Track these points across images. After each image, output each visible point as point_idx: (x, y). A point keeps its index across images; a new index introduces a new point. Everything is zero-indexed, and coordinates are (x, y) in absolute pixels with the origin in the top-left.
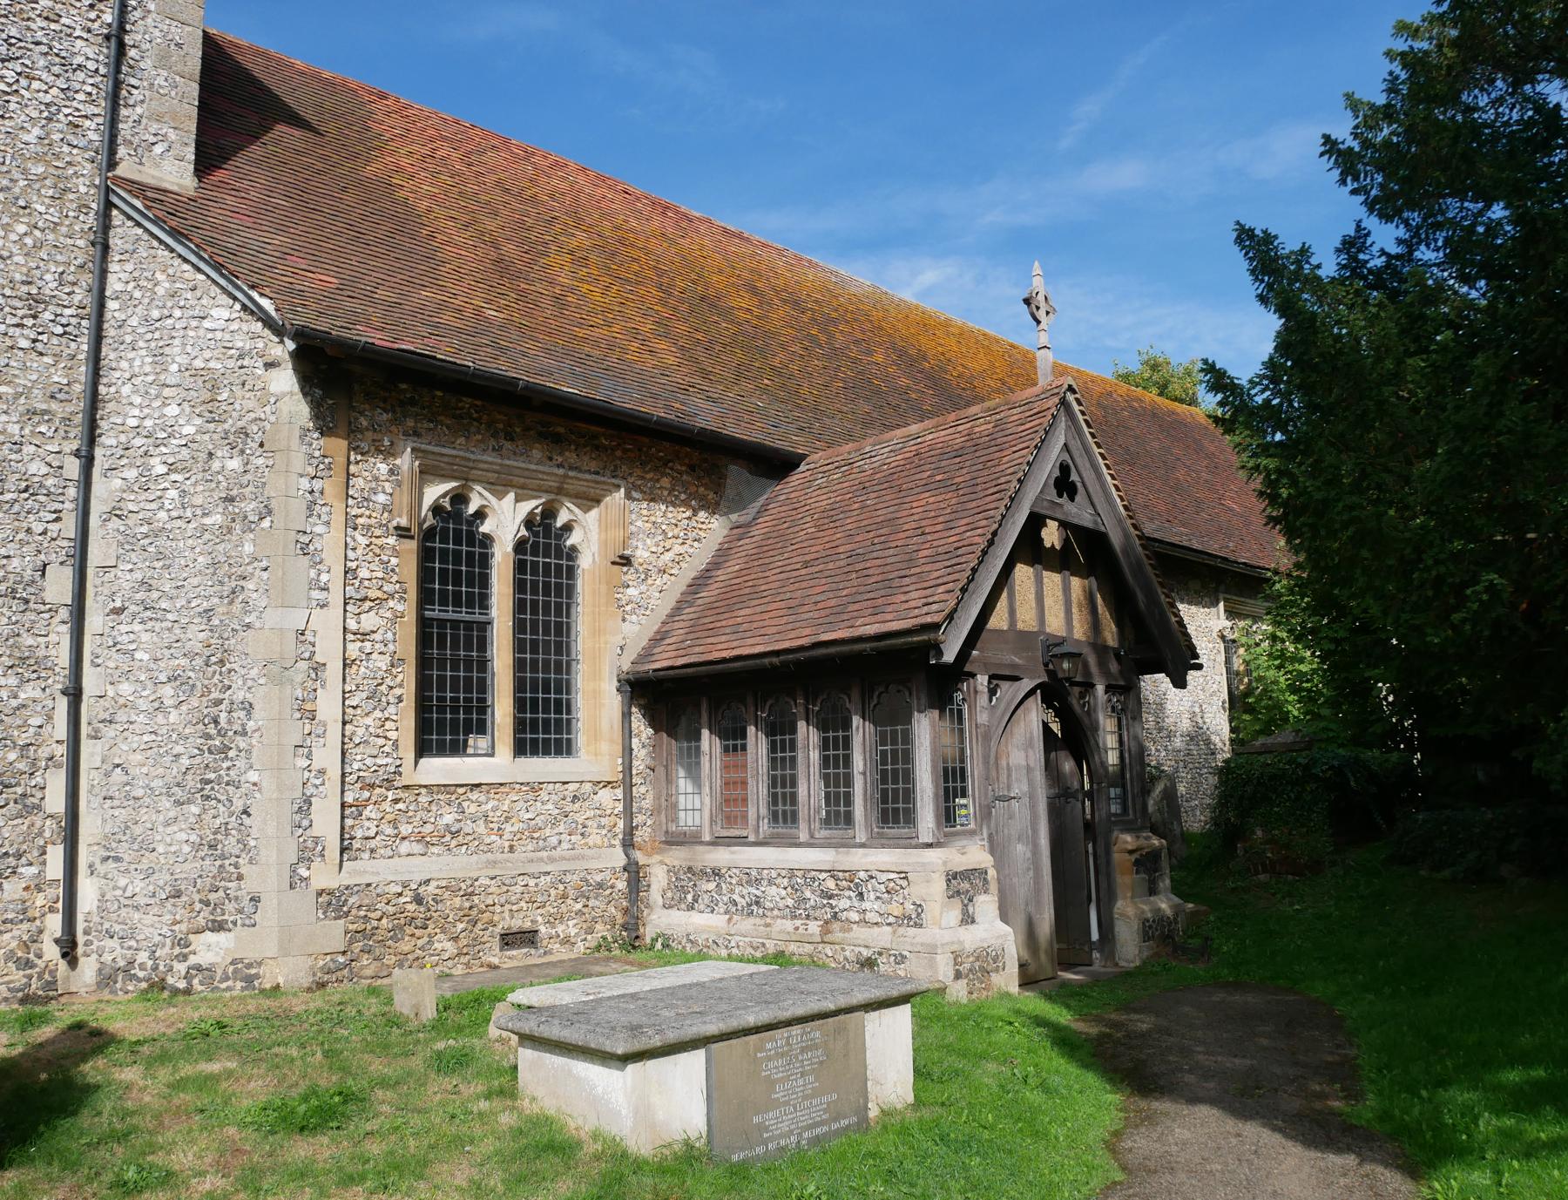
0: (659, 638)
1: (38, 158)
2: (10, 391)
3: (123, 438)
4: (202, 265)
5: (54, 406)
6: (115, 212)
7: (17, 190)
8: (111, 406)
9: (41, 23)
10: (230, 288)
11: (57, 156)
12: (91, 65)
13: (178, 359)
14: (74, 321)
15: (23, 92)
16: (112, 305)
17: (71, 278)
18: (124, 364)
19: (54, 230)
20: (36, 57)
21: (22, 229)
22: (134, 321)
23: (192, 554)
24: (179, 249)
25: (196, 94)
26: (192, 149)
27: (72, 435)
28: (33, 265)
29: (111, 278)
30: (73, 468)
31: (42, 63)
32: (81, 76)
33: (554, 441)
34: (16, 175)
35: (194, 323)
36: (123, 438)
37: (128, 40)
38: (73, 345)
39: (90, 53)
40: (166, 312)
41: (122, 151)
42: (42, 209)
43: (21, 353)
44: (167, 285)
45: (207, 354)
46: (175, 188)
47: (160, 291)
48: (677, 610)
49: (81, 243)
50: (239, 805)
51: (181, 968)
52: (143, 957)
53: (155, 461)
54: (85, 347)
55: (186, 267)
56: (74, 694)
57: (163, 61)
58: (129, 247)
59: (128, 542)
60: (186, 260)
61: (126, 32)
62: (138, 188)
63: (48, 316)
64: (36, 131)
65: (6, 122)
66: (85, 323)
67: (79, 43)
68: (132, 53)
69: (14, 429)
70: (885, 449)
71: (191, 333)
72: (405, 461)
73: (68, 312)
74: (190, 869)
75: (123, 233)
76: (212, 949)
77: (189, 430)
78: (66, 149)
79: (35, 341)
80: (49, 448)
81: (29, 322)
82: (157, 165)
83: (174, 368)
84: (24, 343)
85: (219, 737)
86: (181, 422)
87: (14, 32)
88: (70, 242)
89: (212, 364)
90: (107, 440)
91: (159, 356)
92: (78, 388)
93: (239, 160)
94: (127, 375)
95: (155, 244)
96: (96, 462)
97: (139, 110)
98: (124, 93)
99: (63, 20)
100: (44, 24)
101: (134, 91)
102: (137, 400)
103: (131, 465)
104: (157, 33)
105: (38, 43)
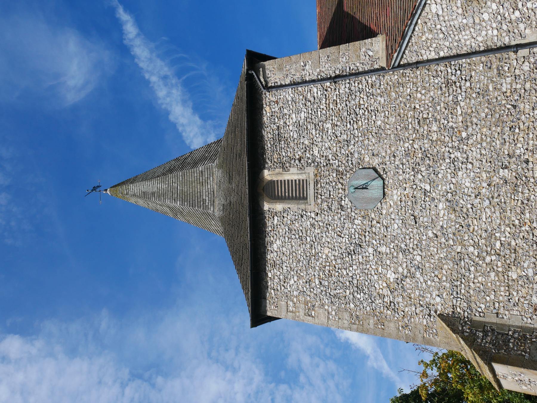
1: (389, 96)
2: (491, 85)
3: (504, 34)
4: (414, 22)
5: (494, 66)
6: (402, 63)
7: (404, 100)
8: (489, 43)
9: (339, 106)
10: (421, 7)
11: (386, 89)
12: (348, 85)
13: (460, 21)
14: (453, 67)
15: (366, 106)
16: (442, 54)
17: (434, 73)
18: (468, 43)
19: (416, 84)
20: (351, 105)
21: (419, 95)
22: (447, 44)
24: (409, 34)
25: (344, 45)
26: (366, 41)
27: (507, 56)
28: (433, 88)
29: (430, 57)
30: (523, 52)
31: (353, 102)
32: (353, 88)
34: (398, 102)
35: (441, 18)
36: (504, 34)
37: (333, 75)
38: (464, 65)
39: (343, 87)
40: (439, 31)
41: (376, 66)
42: (409, 90)
43: (473, 84)
44: (427, 34)
45: (455, 8)
46: (384, 43)
47: (430, 36)
49: (418, 73)
53: (513, 17)
54: (464, 60)
55: (417, 29)
57: (336, 61)
58: (415, 54)
60: (414, 30)
61: (331, 77)
62: (389, 57)
63: (453, 78)
64: (379, 98)
65: (379, 109)
66: (453, 63)
67: (341, 91)
68: (337, 72)
69: (509, 80)
71: (446, 18)
73: (449, 71)
75: (410, 57)
77: (494, 6)
78: (382, 87)
79: (466, 80)
80: (515, 64)
81: (458, 84)
82: (377, 52)
83: (465, 21)
84: (468, 84)
86: (491, 11)
87: (345, 114)
88: (419, 77)
89: (459, 5)
90: (507, 41)
91: (461, 29)
92: (483, 59)
93: (364, 21)
94: (473, 40)
95: (410, 44)
96: (518, 42)
97: (358, 65)
98: (353, 72)
99: (335, 98)
100: (339, 105)
101: (351, 68)
102: (484, 33)
103: (517, 27)
104: (327, 66)
105: (347, 105)
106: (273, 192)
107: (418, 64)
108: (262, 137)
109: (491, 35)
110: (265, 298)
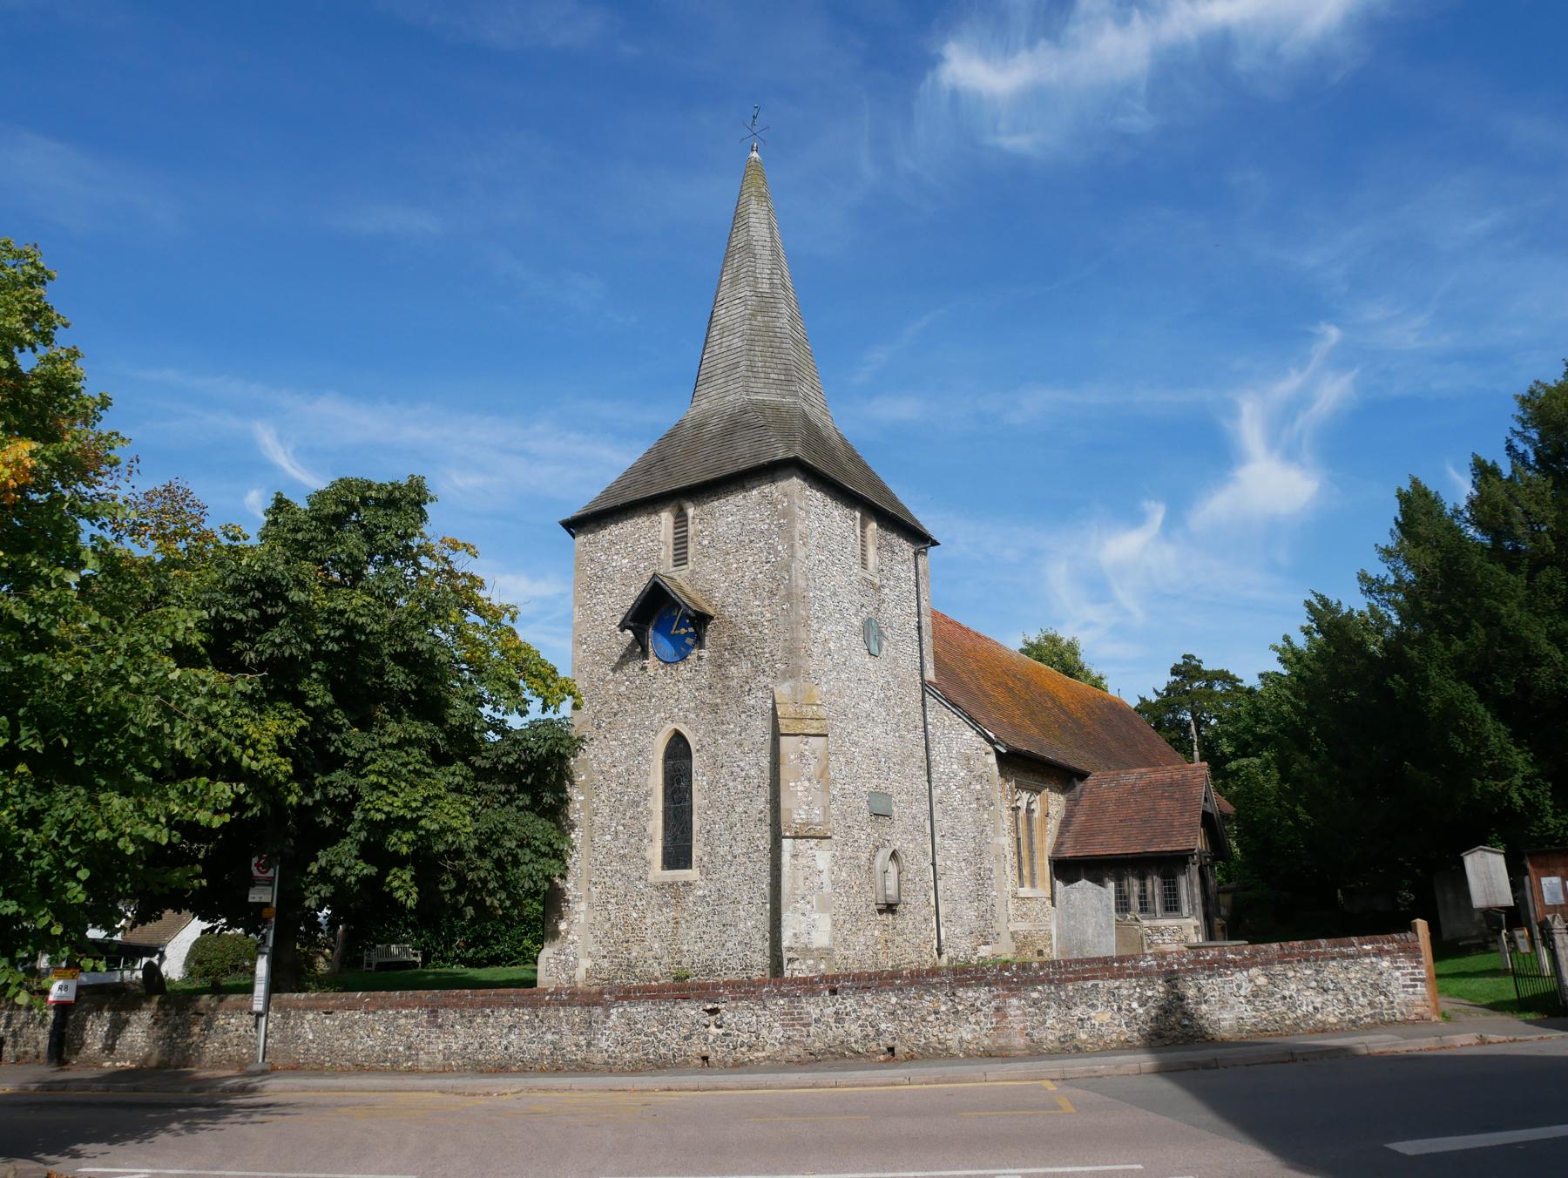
0: (1059, 845)
23: (968, 818)
33: (1033, 771)
39: (915, 633)
48: (1061, 833)
56: (934, 864)
59: (945, 812)
70: (1133, 777)
74: (975, 924)
75: (929, 700)
76: (984, 951)
85: (982, 879)
90: (934, 776)
106: (863, 526)
107: (924, 705)
108: (892, 531)
109: (939, 769)
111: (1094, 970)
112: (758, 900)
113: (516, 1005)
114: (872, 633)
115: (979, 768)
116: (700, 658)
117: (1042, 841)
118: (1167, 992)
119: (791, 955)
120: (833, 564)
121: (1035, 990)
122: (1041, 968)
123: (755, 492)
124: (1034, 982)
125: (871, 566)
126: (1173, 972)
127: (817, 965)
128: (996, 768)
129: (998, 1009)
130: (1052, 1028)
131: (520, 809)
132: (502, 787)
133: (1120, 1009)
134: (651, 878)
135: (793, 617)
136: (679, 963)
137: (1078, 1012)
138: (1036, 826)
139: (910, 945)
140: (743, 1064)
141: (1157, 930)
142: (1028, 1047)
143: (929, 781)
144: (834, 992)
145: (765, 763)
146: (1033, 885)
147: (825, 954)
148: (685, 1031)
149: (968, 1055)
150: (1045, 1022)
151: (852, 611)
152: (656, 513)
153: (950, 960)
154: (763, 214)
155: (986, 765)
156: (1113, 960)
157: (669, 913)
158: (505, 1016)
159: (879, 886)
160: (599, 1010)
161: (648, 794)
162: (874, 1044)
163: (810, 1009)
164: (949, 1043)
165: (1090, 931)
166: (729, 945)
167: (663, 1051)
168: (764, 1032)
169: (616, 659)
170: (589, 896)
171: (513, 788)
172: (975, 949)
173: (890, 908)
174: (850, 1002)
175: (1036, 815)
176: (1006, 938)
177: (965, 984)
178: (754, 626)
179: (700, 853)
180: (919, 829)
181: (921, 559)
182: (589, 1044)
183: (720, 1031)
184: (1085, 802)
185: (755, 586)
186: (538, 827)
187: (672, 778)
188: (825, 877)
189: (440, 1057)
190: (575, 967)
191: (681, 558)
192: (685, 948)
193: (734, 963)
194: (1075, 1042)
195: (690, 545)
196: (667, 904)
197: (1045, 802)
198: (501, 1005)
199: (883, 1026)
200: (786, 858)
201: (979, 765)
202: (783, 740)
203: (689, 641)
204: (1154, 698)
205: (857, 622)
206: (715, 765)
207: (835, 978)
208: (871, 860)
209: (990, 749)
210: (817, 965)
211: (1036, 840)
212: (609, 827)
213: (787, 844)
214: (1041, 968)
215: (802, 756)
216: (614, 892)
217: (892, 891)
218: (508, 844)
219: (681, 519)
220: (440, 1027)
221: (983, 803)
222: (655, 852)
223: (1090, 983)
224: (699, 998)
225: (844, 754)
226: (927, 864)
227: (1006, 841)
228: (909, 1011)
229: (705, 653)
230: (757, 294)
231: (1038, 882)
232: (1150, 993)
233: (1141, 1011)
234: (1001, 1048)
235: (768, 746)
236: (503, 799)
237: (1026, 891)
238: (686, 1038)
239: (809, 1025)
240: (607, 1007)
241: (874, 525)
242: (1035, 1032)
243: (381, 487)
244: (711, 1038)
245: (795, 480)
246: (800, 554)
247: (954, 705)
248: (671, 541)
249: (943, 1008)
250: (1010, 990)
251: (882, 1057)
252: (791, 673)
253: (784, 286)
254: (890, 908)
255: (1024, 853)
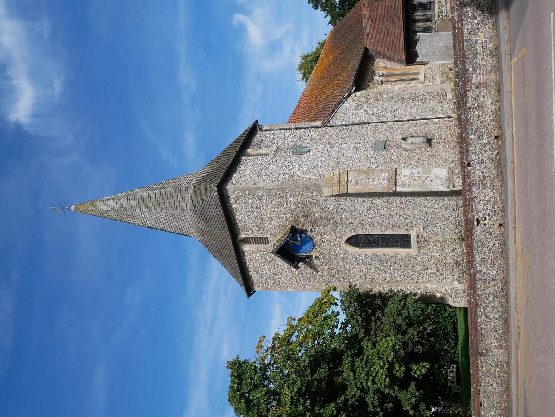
0: (399, 62)
23: (386, 105)
33: (364, 74)
39: (299, 131)
48: (394, 60)
50: (427, 94)
51: (453, 100)
52: (451, 107)
56: (408, 121)
59: (383, 116)
70: (367, 26)
72: (370, 83)
74: (437, 101)
76: (450, 96)
77: (365, 108)
85: (416, 98)
90: (366, 121)
91: (353, 114)
106: (249, 155)
107: (333, 126)
108: (251, 142)
110: (228, 183)
111: (459, 41)
112: (425, 203)
113: (476, 315)
114: (299, 151)
115: (363, 100)
116: (312, 231)
117: (397, 69)
118: (470, 6)
119: (451, 187)
120: (267, 169)
121: (468, 69)
122: (458, 67)
123: (234, 206)
124: (464, 70)
125: (268, 152)
126: (460, 3)
127: (456, 174)
128: (363, 92)
129: (477, 87)
130: (487, 61)
131: (383, 315)
132: (373, 323)
133: (478, 29)
134: (415, 253)
135: (292, 187)
136: (455, 240)
137: (479, 49)
138: (390, 72)
139: (447, 131)
140: (503, 207)
141: (440, 13)
142: (495, 72)
143: (369, 123)
144: (469, 165)
145: (360, 200)
146: (418, 73)
147: (451, 170)
148: (488, 235)
149: (499, 101)
150: (483, 65)
151: (289, 160)
152: (243, 252)
153: (454, 112)
154: (101, 204)
155: (361, 96)
156: (454, 33)
157: (432, 244)
158: (481, 320)
159: (418, 146)
160: (478, 276)
161: (375, 255)
162: (494, 146)
163: (477, 176)
164: (493, 110)
165: (441, 45)
166: (447, 216)
167: (497, 245)
168: (488, 197)
169: (312, 271)
170: (424, 282)
171: (373, 318)
172: (449, 100)
173: (429, 141)
174: (474, 157)
175: (385, 72)
176: (443, 86)
177: (465, 103)
178: (296, 205)
179: (403, 230)
180: (391, 128)
181: (264, 128)
182: (494, 280)
183: (488, 218)
184: (379, 49)
185: (279, 206)
186: (392, 306)
187: (368, 244)
188: (415, 171)
189: (501, 351)
190: (458, 289)
191: (265, 241)
192: (448, 237)
193: (455, 213)
194: (493, 50)
195: (258, 236)
196: (427, 246)
197: (378, 68)
198: (476, 322)
199: (485, 141)
200: (405, 189)
201: (361, 100)
202: (350, 191)
203: (303, 236)
204: (329, 18)
205: (294, 158)
206: (361, 223)
207: (462, 164)
208: (406, 150)
209: (353, 95)
210: (456, 174)
211: (397, 72)
212: (391, 273)
213: (399, 189)
214: (458, 67)
215: (357, 182)
216: (422, 271)
217: (421, 140)
218: (400, 321)
219: (246, 241)
220: (487, 351)
221: (379, 97)
222: (402, 251)
223: (465, 43)
224: (472, 228)
225: (356, 163)
226: (408, 124)
227: (397, 87)
228: (478, 129)
229: (309, 229)
230: (140, 205)
231: (417, 71)
232: (470, 14)
233: (479, 19)
234: (496, 85)
235: (353, 199)
236: (379, 323)
237: (421, 77)
238: (491, 234)
239: (484, 176)
240: (476, 272)
241: (249, 151)
242: (488, 69)
243: (232, 382)
244: (491, 222)
245: (228, 187)
246: (262, 184)
247: (333, 112)
248: (257, 245)
249: (477, 113)
250: (468, 81)
251: (500, 142)
252: (318, 188)
253: (135, 194)
254: (429, 141)
255: (403, 78)
